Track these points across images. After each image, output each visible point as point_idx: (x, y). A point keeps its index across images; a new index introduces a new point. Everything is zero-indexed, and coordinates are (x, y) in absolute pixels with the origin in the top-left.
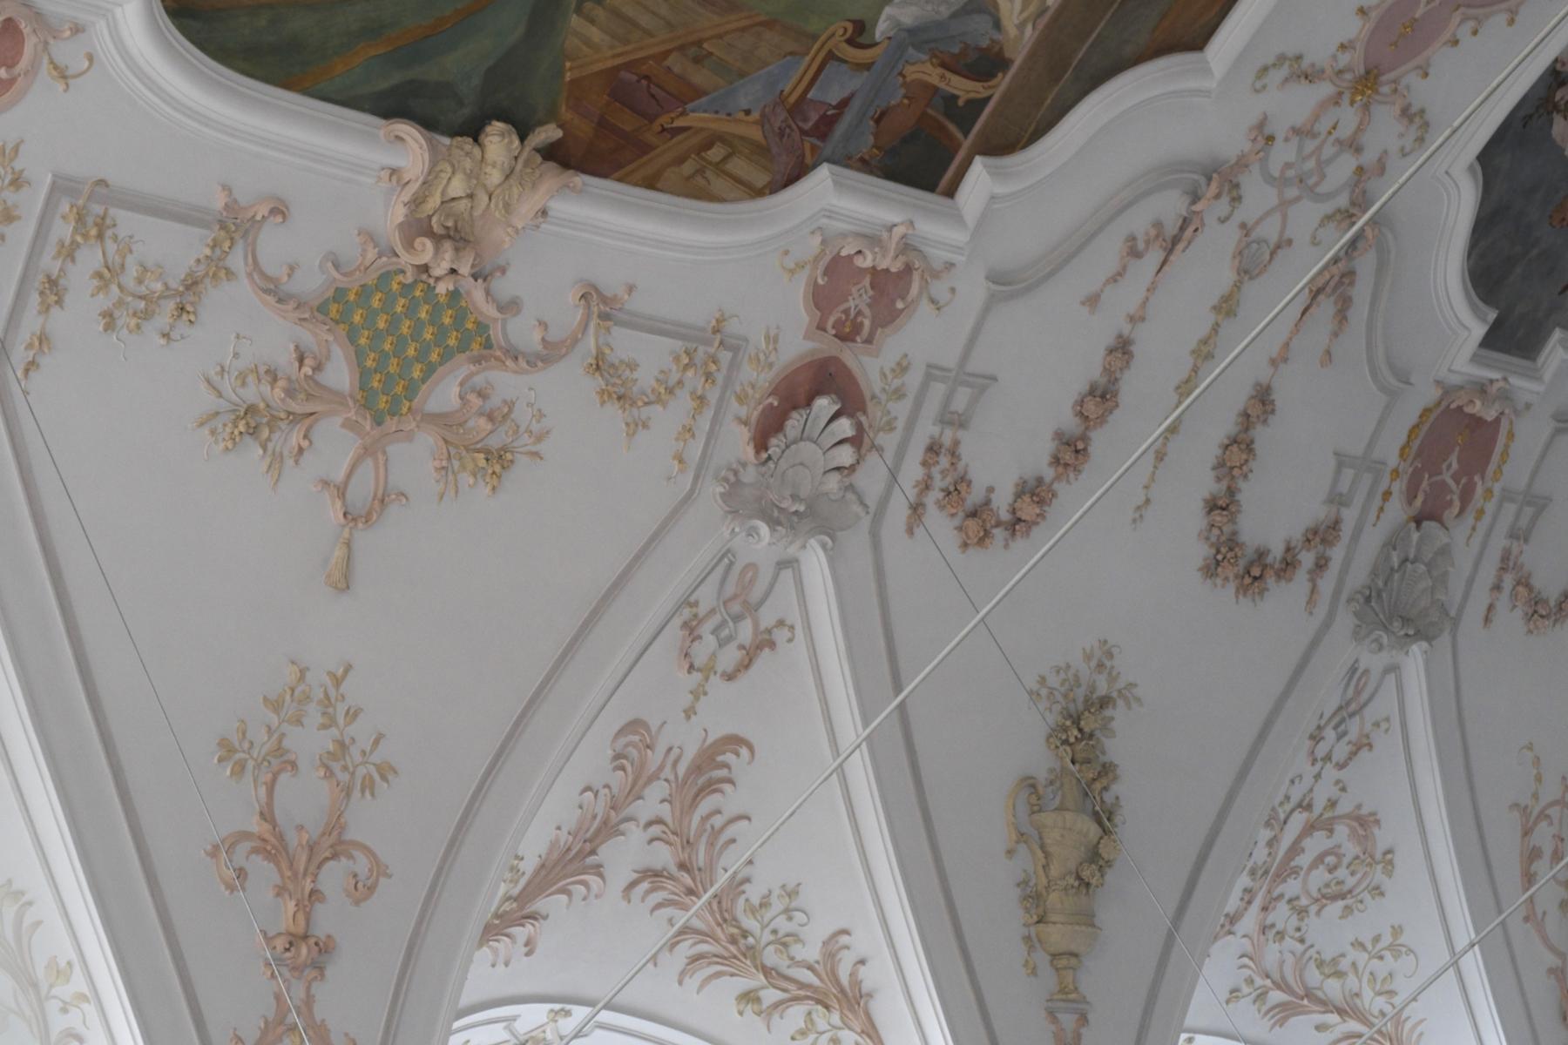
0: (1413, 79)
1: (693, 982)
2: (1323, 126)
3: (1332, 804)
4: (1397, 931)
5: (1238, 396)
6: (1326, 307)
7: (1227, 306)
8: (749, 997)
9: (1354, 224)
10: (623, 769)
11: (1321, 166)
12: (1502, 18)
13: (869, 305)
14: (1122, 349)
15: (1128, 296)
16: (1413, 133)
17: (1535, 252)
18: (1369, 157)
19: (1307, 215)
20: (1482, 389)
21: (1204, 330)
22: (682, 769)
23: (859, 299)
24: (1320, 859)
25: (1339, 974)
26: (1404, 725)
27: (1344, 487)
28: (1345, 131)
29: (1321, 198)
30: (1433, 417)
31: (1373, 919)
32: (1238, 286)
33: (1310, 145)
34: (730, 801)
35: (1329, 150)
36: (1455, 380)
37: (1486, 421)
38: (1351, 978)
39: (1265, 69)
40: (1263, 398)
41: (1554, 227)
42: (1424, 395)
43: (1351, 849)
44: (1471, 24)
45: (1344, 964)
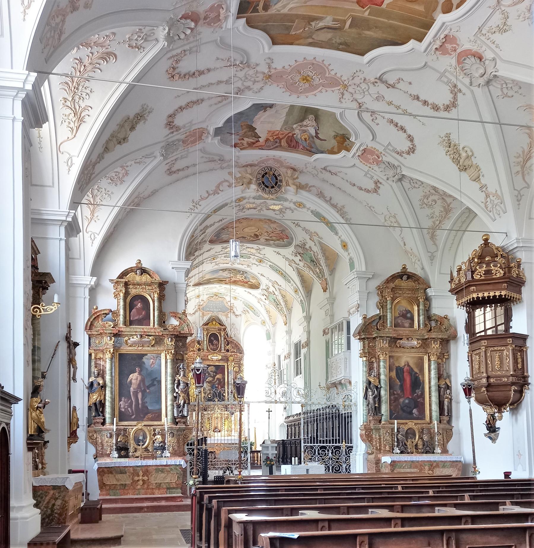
0: (269, 83)
1: (61, 86)
2: (258, 75)
3: (127, 166)
4: (112, 193)
5: (200, 97)
6: (220, 99)
7: (219, 82)
8: (65, 99)
10: (104, 38)
11: (250, 80)
13: (211, 18)
14: (209, 70)
15: (219, 64)
16: (257, 91)
18: (252, 87)
19: (239, 84)
20: (209, 133)
21: (213, 82)
22: (107, 50)
23: (212, 15)
24: (116, 172)
25: (98, 191)
26: (146, 166)
27: (187, 125)
28: (257, 79)
29: (243, 84)
31: (112, 188)
32: (223, 82)
33: (254, 76)
34: (104, 64)
35: (253, 79)
36: (209, 128)
38: (99, 193)
39: (270, 58)
40: (202, 100)
42: (204, 126)
43: (121, 176)
44: (283, 86)
45: (101, 190)
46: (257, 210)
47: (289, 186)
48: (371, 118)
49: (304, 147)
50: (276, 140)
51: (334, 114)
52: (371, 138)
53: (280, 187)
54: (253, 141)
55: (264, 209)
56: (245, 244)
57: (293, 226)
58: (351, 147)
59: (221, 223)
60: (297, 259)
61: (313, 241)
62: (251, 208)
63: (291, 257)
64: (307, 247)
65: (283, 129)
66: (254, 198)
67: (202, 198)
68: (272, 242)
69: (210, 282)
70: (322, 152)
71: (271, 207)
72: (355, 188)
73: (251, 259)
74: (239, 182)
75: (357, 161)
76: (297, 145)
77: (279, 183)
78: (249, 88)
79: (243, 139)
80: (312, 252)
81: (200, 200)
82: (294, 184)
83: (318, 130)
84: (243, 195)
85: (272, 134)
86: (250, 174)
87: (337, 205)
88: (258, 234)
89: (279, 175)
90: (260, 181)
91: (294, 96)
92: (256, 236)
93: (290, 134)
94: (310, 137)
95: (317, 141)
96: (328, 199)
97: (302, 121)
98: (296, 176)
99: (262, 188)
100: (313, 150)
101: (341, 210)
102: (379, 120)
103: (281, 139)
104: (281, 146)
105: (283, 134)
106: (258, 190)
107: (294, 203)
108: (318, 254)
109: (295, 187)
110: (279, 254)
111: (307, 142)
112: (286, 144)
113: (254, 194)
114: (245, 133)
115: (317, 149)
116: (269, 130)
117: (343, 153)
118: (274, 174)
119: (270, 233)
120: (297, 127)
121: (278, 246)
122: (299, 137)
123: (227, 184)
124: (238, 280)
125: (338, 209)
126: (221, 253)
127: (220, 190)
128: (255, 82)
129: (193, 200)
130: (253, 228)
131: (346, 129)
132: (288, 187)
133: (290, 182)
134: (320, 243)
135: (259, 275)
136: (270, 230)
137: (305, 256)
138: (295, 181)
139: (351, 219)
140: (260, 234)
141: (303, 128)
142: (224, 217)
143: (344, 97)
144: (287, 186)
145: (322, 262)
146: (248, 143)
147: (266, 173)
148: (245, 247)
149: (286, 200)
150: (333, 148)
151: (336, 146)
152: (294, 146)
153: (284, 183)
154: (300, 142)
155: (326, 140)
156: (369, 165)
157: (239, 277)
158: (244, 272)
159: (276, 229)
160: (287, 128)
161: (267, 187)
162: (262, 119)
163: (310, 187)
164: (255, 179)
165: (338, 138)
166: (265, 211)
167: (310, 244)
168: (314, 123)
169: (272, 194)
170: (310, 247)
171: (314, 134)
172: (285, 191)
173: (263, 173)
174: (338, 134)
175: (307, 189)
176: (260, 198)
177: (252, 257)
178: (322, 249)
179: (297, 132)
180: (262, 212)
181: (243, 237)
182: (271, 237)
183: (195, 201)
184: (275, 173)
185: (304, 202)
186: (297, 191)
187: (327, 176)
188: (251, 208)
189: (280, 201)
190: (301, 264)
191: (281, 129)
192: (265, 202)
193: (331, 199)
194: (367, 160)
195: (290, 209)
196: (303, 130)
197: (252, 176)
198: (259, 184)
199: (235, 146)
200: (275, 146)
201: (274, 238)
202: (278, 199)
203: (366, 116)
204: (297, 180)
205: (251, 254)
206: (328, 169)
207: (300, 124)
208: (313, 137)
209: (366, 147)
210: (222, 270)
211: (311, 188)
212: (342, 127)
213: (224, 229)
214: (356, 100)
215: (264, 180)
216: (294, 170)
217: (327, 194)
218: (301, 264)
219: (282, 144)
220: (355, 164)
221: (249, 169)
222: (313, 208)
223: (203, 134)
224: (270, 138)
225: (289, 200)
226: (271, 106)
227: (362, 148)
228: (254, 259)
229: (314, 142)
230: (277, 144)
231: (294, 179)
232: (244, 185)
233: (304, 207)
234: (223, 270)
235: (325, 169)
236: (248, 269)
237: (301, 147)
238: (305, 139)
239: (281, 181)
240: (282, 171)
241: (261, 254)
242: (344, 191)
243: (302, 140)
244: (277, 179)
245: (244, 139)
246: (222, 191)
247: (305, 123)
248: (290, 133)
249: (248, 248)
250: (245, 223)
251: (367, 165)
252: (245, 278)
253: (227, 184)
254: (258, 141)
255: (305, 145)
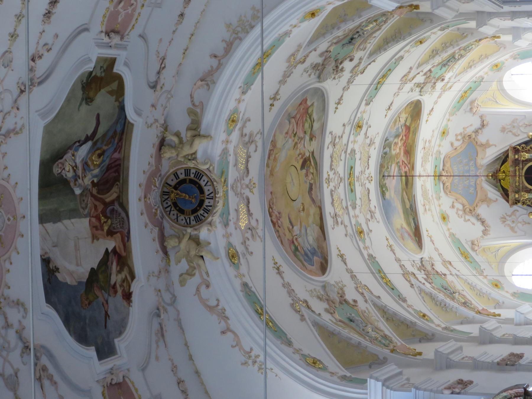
0: (7, 292)
6: (46, 383)
9: (30, 349)
12: (14, 254)
16: (22, 310)
17: (87, 321)
18: (16, 326)
20: (111, 372)
30: (106, 392)
37: (121, 382)
41: (85, 309)
46: (250, 195)
47: (195, 153)
48: (46, 54)
49: (115, 151)
50: (108, 215)
51: (48, 131)
52: (85, 34)
53: (199, 174)
54: (115, 264)
55: (247, 181)
56: (325, 176)
57: (278, 104)
58: (105, 60)
59: (284, 268)
60: (348, 65)
61: (308, 56)
62: (248, 210)
63: (346, 75)
64: (320, 60)
65: (86, 211)
66: (226, 225)
67: (237, 345)
68: (316, 126)
69: (411, 206)
70: (122, 108)
71: (242, 167)
72: (187, 12)
73: (356, 147)
74: (199, 266)
75: (133, 36)
76: (113, 165)
77: (192, 176)
78: (19, 334)
79: (114, 287)
80: (332, 49)
81: (241, 348)
82: (191, 144)
83: (79, 142)
84: (223, 253)
85: (97, 229)
86: (180, 239)
87: (226, 42)
88: (301, 161)
89: (176, 175)
90: (192, 218)
91: (23, 226)
92: (305, 163)
93: (95, 191)
94: (95, 148)
95: (101, 131)
96: (214, 62)
97: (65, 182)
98: (175, 139)
99: (206, 215)
100: (119, 128)
101: (235, 32)
102: (48, 38)
103: (106, 205)
104: (118, 198)
105: (96, 207)
106: (210, 224)
107: (229, 133)
108: (334, 39)
109: (197, 141)
110: (341, 99)
111: (105, 148)
112: (115, 189)
113: (219, 230)
114: (101, 288)
115: (117, 122)
116: (90, 240)
117: (119, 68)
118: (176, 188)
119: (296, 140)
120: (80, 186)
121: (324, 109)
122: (96, 171)
123: (203, 289)
124: (402, 148)
125: (235, 39)
126: (347, 222)
127: (218, 305)
128: (8, 326)
129: (242, 364)
130: (289, 180)
131: (73, 90)
132: (199, 155)
133: (187, 151)
134: (311, 42)
135: (390, 113)
136: (291, 142)
137: (340, 57)
138: (184, 140)
139: (253, 8)
140: (302, 157)
141: (80, 172)
142: (270, 264)
143: (12, 127)
144: (195, 159)
145: (351, 25)
146: (119, 272)
147: (175, 204)
148: (331, 173)
149: (225, 152)
150: (111, 93)
151: (108, 88)
152: (115, 172)
153: (191, 165)
154: (107, 162)
155: (98, 116)
156: (138, 10)
157: (397, 150)
158: (387, 144)
159: (287, 133)
160: (83, 206)
161: (202, 202)
162: (72, 267)
163: (194, 105)
164: (189, 230)
165: (91, 94)
166: (250, 177)
167: (314, 58)
168: (68, 156)
169: (215, 192)
170: (321, 55)
171: (90, 144)
172: (206, 164)
173: (175, 212)
174: (83, 99)
175: (198, 110)
176: (226, 213)
177: (350, 146)
178: (323, 35)
179: (87, 181)
180: (256, 180)
181: (311, 189)
182: (305, 133)
183: (243, 359)
184: (173, 183)
185: (226, 115)
186: (205, 137)
187: (167, 76)
188: (248, 210)
189: (228, 163)
190: (358, 55)
191: (86, 216)
192: (232, 188)
193: (215, 57)
194: (129, 18)
195: (241, 129)
196: (84, 169)
197: (184, 235)
198: (199, 221)
199: (128, 296)
200: (120, 210)
201: (307, 125)
202: (223, 173)
203: (42, 66)
204: (183, 135)
205: (346, 152)
206: (153, 78)
207: (72, 184)
208: (95, 144)
209: (103, 34)
210: (383, 194)
211: (197, 103)
212: (68, 100)
213: (296, 249)
214: (16, 101)
215: (188, 208)
216: (162, 144)
217: (207, 63)
218: (358, 55)
219: (115, 196)
220: (140, 36)
221: (171, 243)
222: (236, 93)
223: (114, 382)
224: (106, 228)
225: (224, 146)
226: (46, 261)
227: (106, 40)
228: (355, 142)
229: (104, 136)
230: (117, 207)
231: (181, 142)
232: (203, 254)
233: (236, 111)
234: (383, 189)
235: (154, 86)
236: (378, 141)
237: (116, 155)
238: (99, 156)
239: (187, 171)
240: (166, 168)
241: (344, 132)
242: (195, 26)
243: (103, 161)
244: (183, 181)
245: (112, 282)
246: (218, 300)
247: (70, 175)
248: (92, 195)
249: (331, 165)
250: (281, 206)
251: (139, 14)
252: (397, 136)
253: (203, 289)
254: (114, 250)
255: (112, 150)
